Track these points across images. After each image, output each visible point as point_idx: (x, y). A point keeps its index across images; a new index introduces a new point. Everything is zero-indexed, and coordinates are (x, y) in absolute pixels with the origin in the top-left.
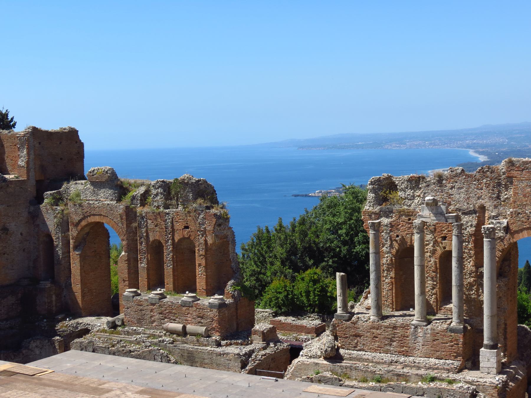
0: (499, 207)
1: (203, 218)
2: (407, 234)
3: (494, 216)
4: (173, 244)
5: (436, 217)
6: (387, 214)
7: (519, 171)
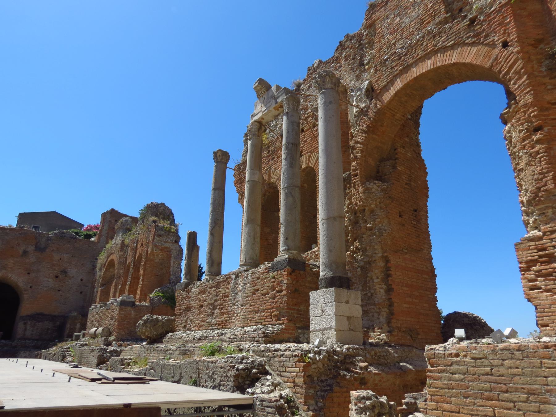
4: (134, 262)
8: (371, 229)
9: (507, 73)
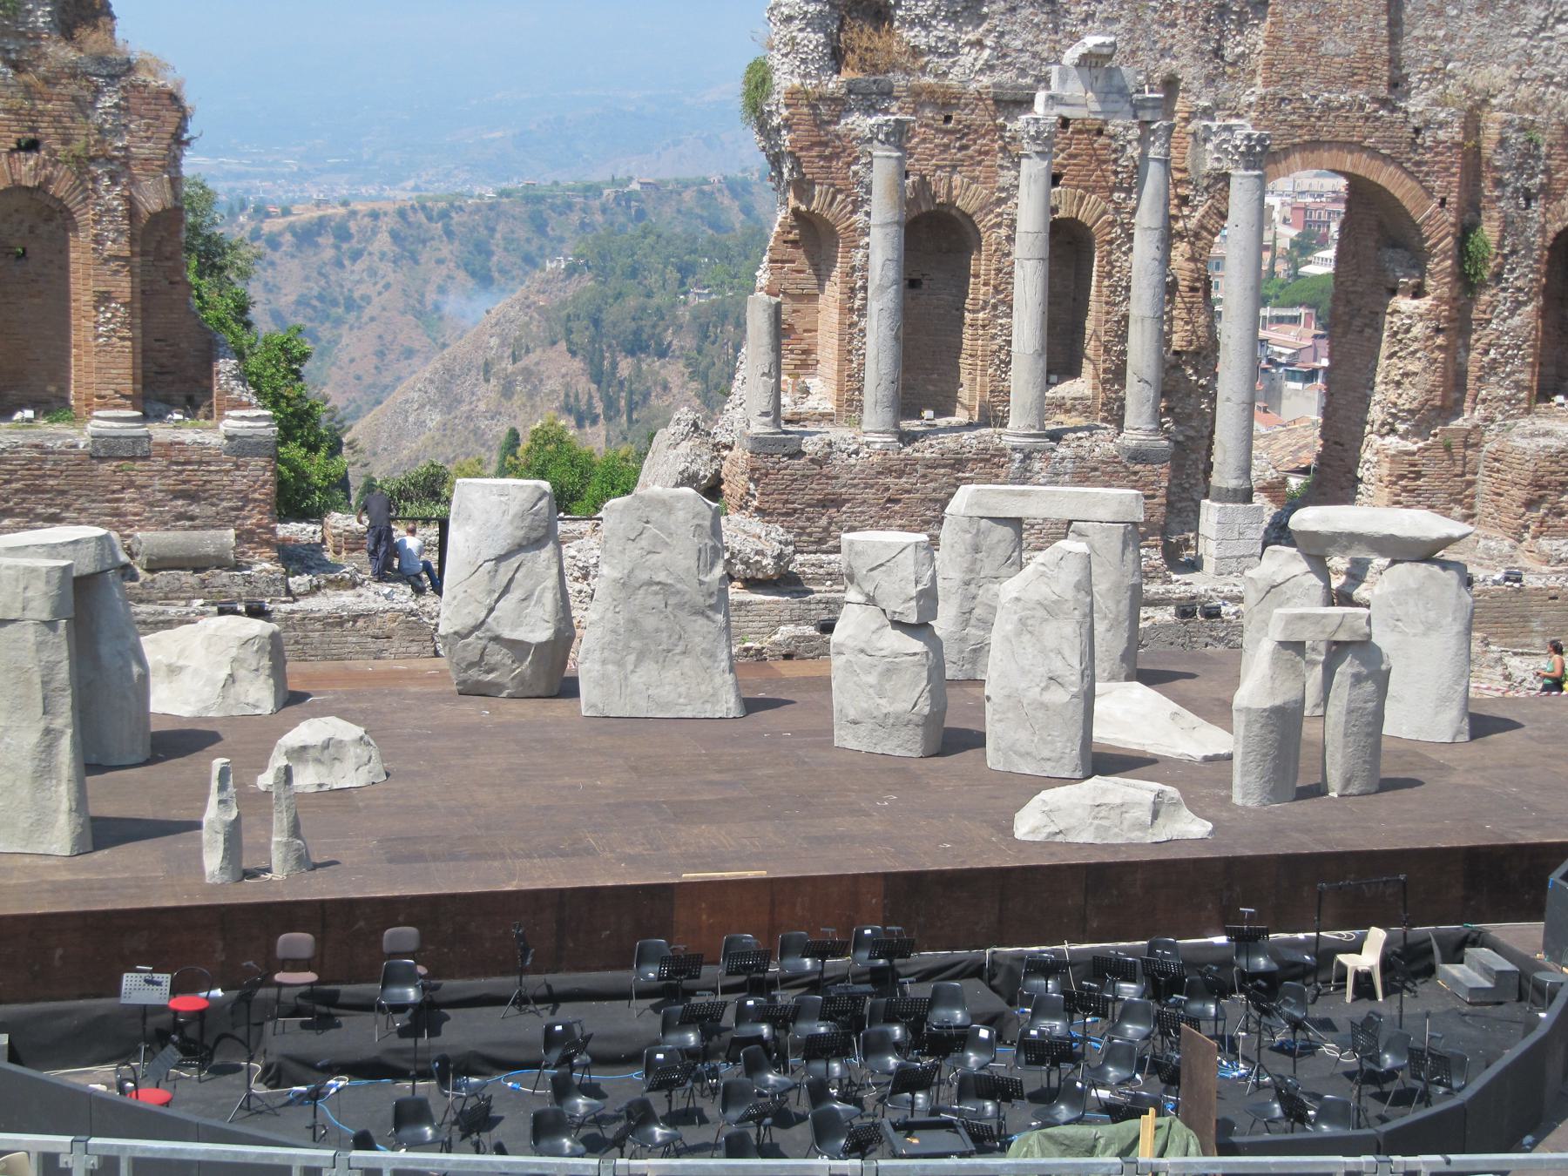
0: (1219, 82)
1: (116, 106)
2: (938, 167)
3: (1205, 109)
5: (1102, 102)
6: (871, 98)
8: (1202, 386)
9: (1435, 245)
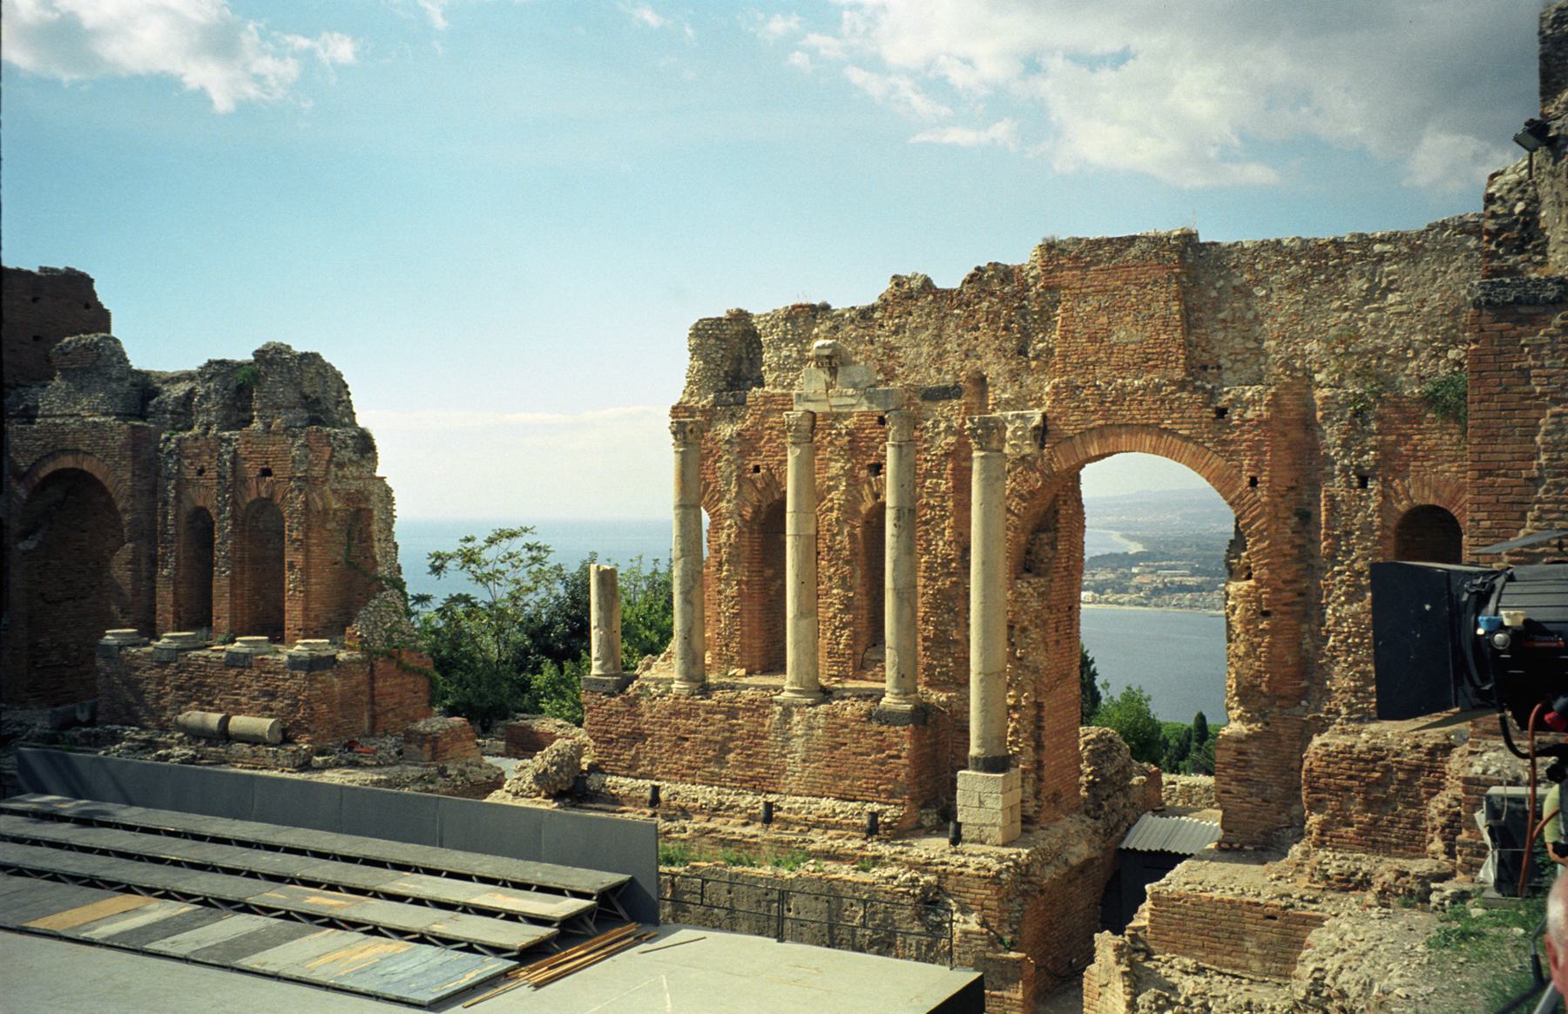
3: (1007, 402)
4: (233, 516)
7: (1077, 268)
